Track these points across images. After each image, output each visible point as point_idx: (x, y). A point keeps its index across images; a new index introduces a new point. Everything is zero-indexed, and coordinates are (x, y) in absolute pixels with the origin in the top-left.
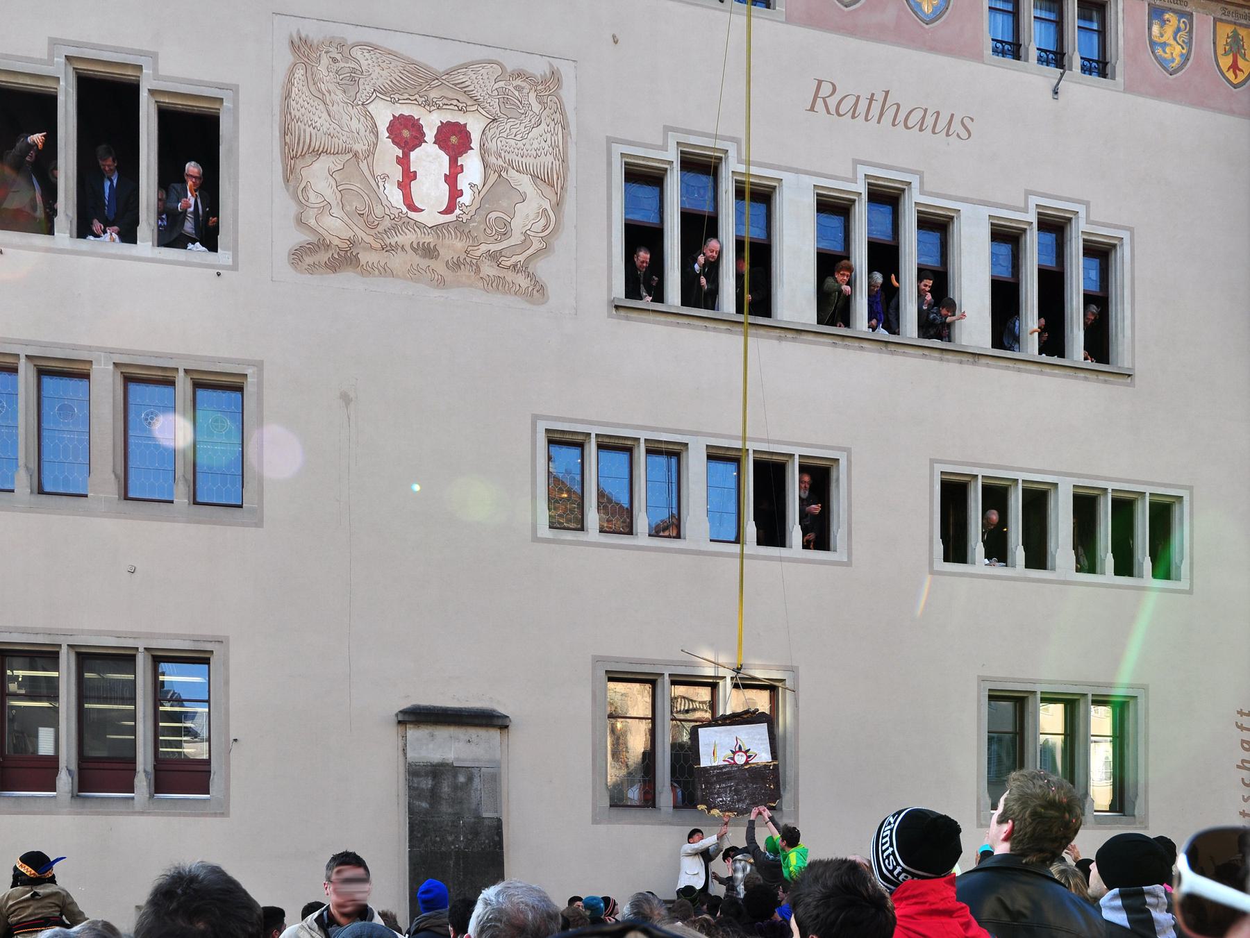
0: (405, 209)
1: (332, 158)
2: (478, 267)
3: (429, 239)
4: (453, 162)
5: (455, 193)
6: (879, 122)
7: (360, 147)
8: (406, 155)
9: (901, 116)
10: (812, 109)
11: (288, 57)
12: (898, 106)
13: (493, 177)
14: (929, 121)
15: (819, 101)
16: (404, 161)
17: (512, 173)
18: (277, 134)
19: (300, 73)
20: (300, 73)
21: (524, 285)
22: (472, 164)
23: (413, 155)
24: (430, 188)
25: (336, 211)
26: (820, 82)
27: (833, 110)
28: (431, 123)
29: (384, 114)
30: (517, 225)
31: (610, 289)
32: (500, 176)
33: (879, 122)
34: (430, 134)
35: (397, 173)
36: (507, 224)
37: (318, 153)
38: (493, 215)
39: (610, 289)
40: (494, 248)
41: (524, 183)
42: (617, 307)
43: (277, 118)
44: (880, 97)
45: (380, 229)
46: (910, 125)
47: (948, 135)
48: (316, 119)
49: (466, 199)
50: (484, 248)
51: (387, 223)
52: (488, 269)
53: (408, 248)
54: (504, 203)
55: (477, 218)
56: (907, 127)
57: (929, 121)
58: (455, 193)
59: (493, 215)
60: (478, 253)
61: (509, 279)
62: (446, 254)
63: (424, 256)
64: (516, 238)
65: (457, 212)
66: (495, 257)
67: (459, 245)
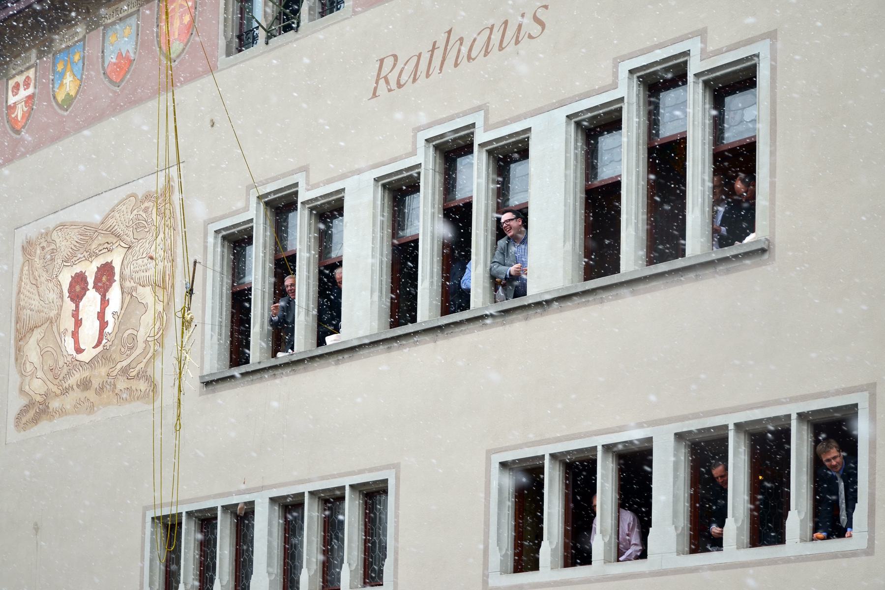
0: (74, 353)
1: (39, 330)
2: (115, 385)
3: (86, 374)
4: (103, 297)
5: (103, 324)
6: (441, 69)
7: (53, 314)
8: (77, 307)
9: (464, 50)
10: (374, 95)
11: (19, 257)
12: (461, 40)
13: (128, 298)
14: (496, 37)
15: (382, 82)
16: (76, 314)
17: (140, 288)
18: (13, 324)
19: (26, 268)
20: (26, 268)
21: (143, 389)
22: (115, 294)
23: (81, 304)
24: (90, 330)
25: (40, 374)
26: (382, 61)
27: (393, 85)
28: (90, 270)
29: (65, 278)
30: (142, 335)
31: (202, 368)
32: (132, 295)
33: (441, 69)
34: (91, 281)
35: (70, 324)
36: (134, 338)
37: (32, 330)
38: (126, 335)
39: (202, 368)
40: (125, 363)
41: (146, 294)
42: (208, 384)
43: (13, 312)
44: (441, 44)
45: (61, 378)
46: (473, 55)
47: (517, 42)
48: (32, 302)
49: (109, 329)
50: (119, 366)
51: (65, 370)
52: (122, 384)
53: (75, 387)
54: (133, 320)
55: (116, 342)
56: (469, 58)
57: (496, 37)
58: (103, 324)
59: (126, 335)
60: (115, 373)
61: (134, 388)
62: (96, 383)
63: (83, 390)
64: (141, 345)
65: (104, 341)
66: (125, 371)
67: (103, 371)
